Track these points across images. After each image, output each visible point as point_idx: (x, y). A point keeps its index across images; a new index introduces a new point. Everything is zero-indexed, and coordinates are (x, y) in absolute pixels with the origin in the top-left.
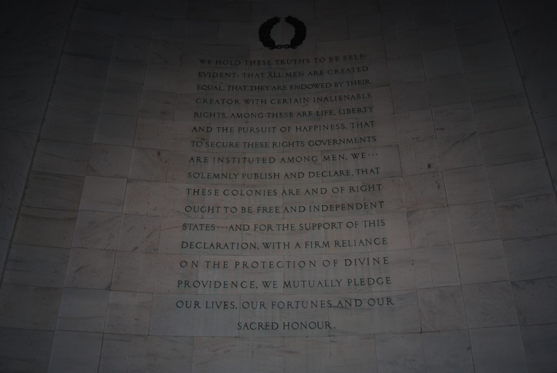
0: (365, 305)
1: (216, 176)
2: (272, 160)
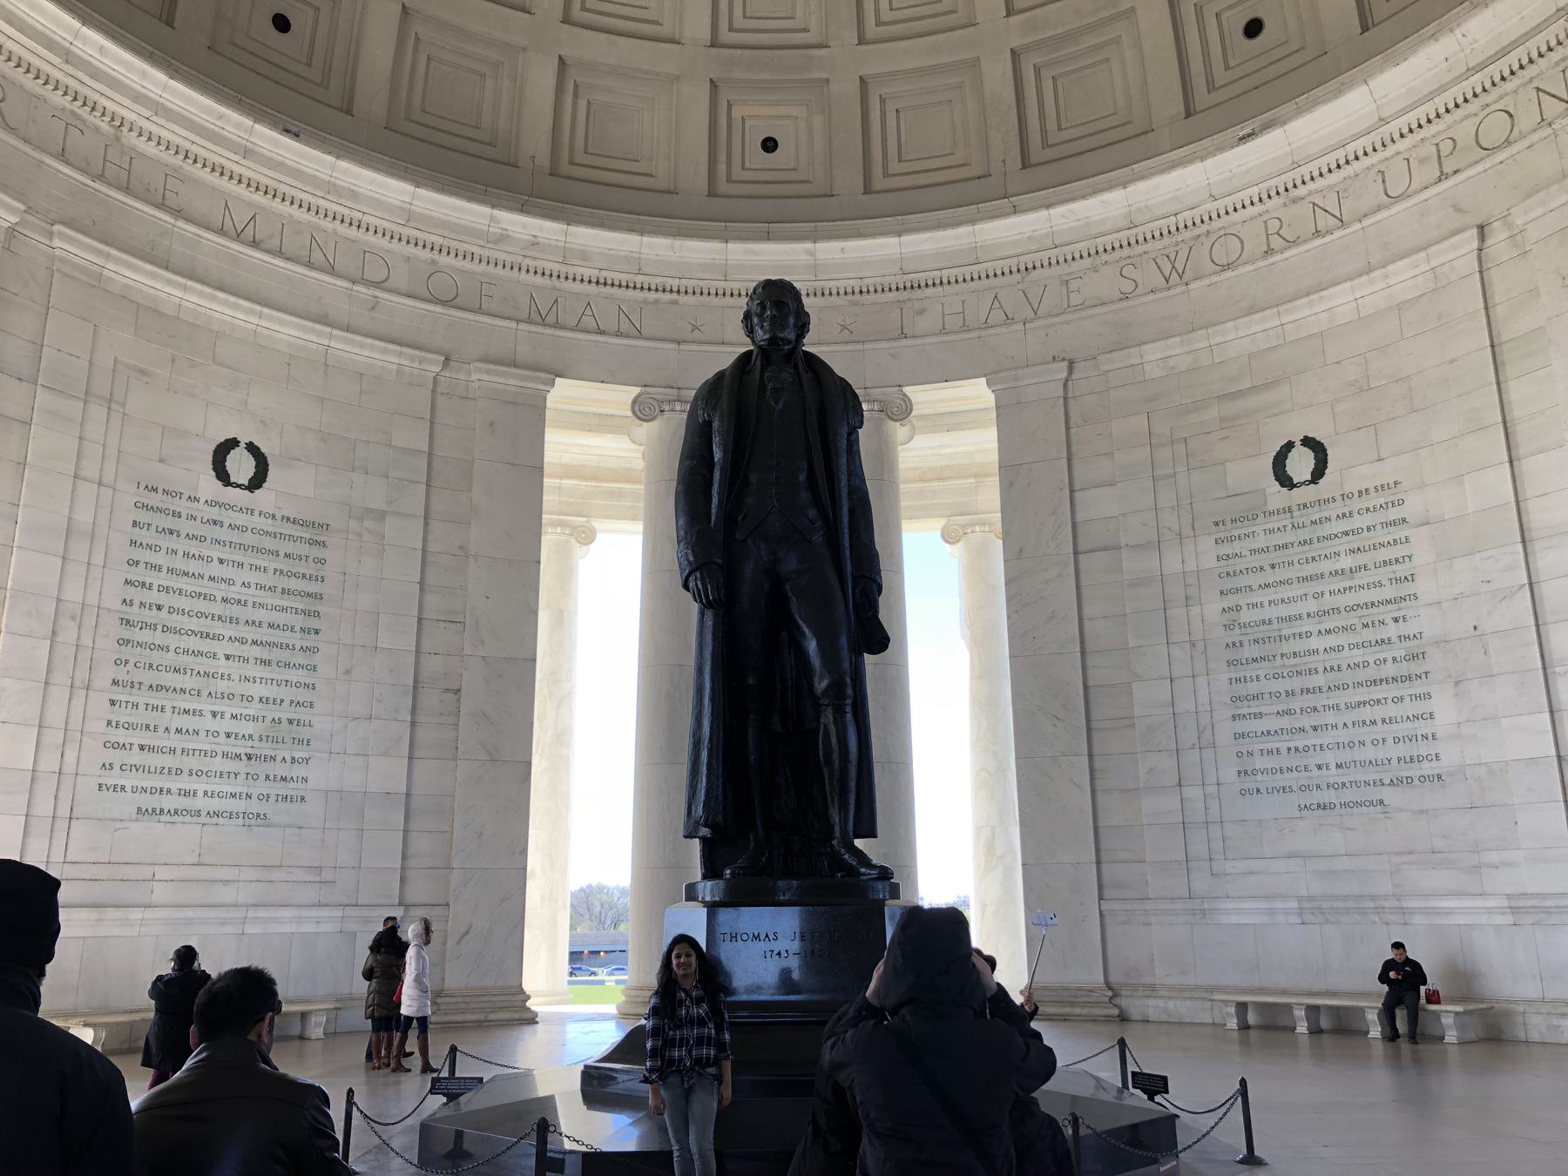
0: (1416, 782)
1: (1255, 660)
2: (1309, 634)
